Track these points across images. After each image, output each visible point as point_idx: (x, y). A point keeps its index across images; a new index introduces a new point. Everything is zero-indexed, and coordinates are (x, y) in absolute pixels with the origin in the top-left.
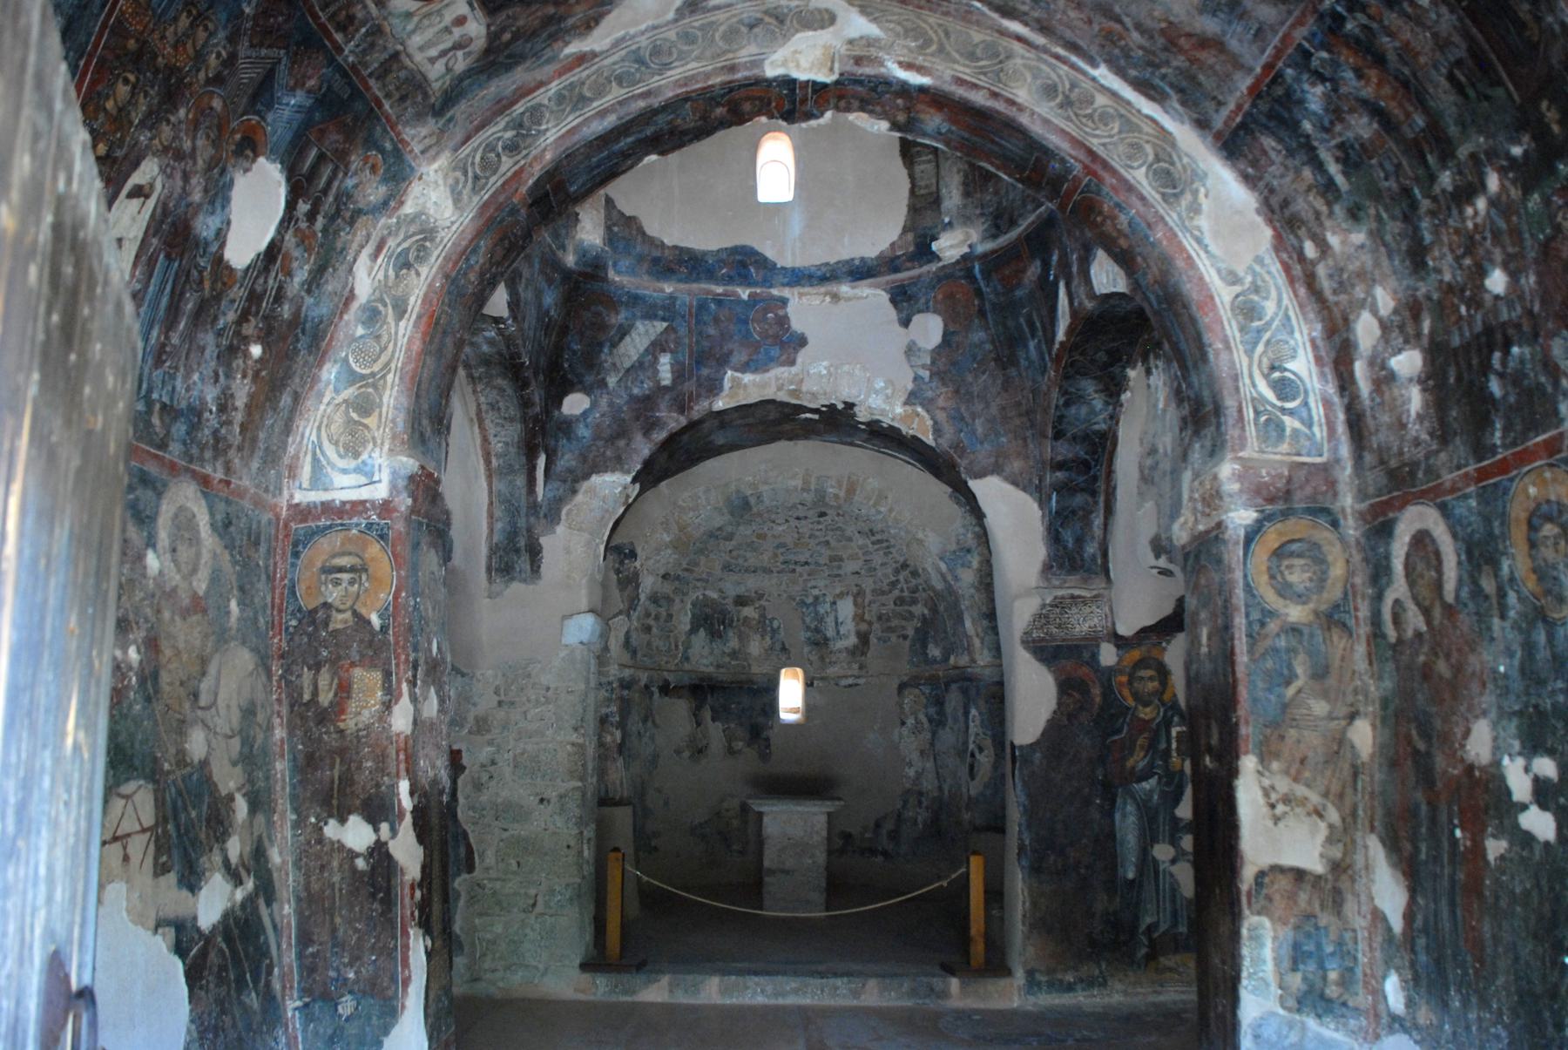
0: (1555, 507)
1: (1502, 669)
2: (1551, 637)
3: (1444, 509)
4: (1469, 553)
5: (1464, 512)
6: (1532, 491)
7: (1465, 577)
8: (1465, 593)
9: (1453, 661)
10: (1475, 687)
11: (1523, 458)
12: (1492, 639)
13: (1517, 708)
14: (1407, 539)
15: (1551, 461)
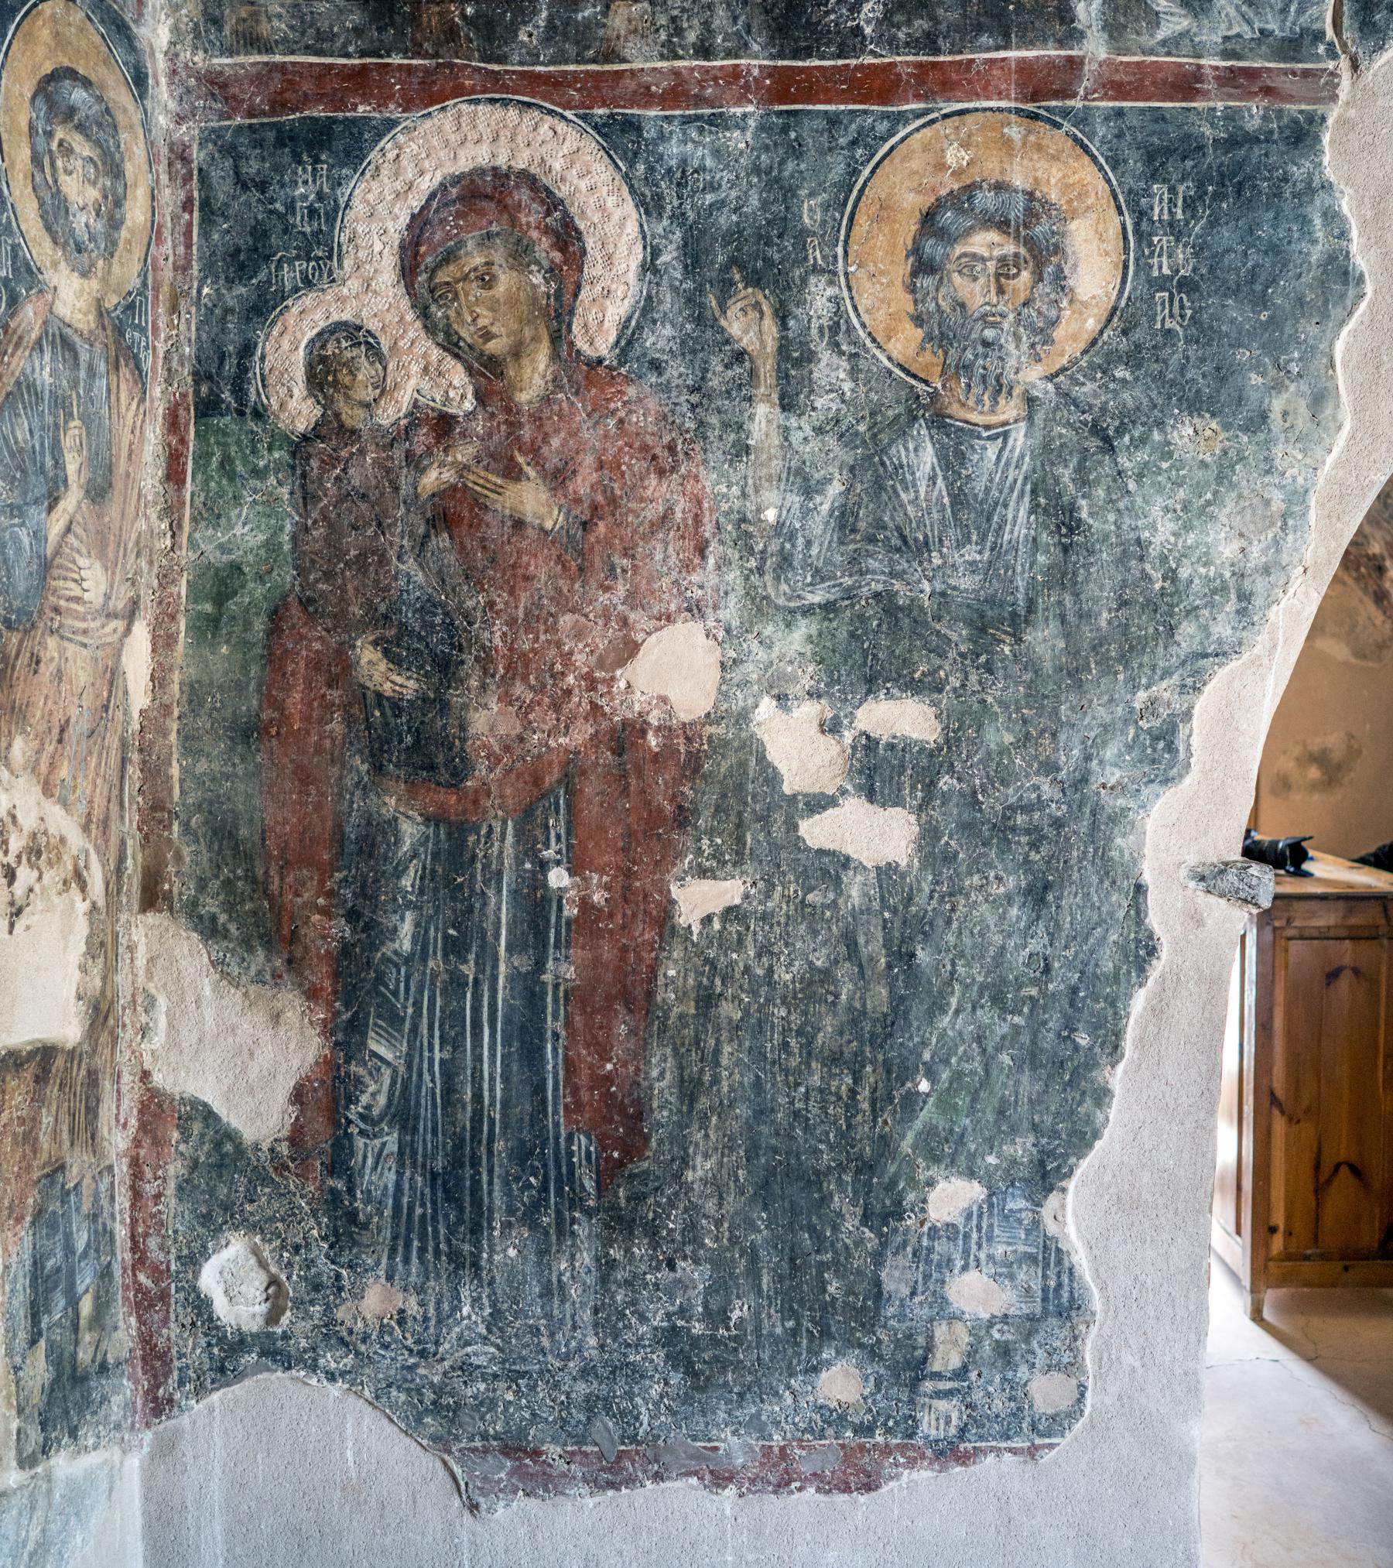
0: (1020, 202)
1: (770, 515)
2: (953, 460)
3: (620, 137)
4: (693, 257)
5: (700, 154)
6: (955, 156)
7: (667, 302)
8: (659, 339)
9: (583, 483)
10: (663, 554)
11: (937, 82)
12: (743, 450)
13: (817, 598)
14: (427, 184)
15: (1030, 107)
